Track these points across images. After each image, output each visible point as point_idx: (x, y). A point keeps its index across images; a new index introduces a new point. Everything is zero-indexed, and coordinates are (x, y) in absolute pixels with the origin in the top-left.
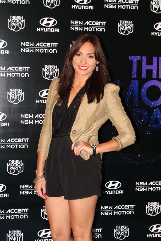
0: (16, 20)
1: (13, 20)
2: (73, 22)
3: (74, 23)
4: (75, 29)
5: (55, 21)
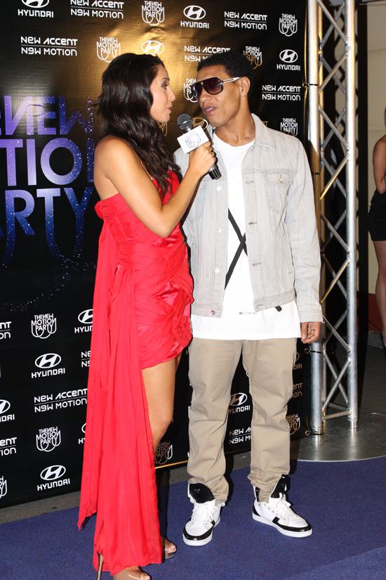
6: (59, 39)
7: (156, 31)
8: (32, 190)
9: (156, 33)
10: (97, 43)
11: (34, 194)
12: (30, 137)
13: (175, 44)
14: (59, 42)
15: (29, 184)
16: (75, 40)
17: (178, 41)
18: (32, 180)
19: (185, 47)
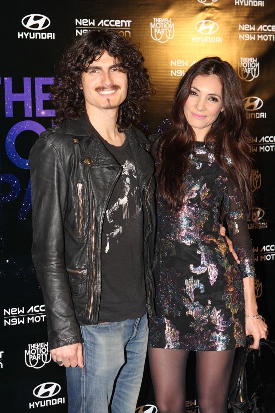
2: (80, 21)
3: (81, 24)
5: (47, 20)
6: (113, 21)
7: (210, 10)
9: (211, 12)
10: (152, 23)
13: (229, 23)
14: (113, 23)
16: (130, 21)
17: (233, 20)
19: (240, 26)
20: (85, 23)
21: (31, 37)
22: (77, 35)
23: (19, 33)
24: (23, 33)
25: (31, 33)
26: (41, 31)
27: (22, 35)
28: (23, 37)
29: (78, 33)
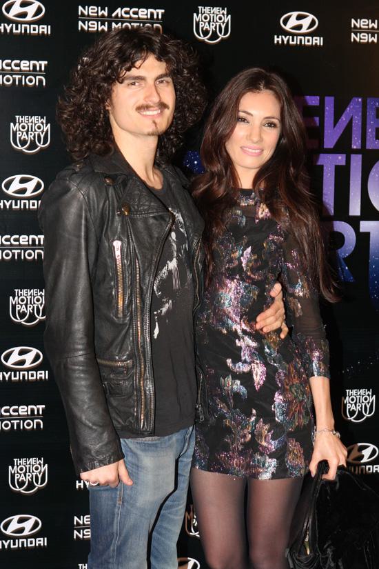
0: (212, 15)
1: (204, 15)
2: (357, 22)
4: (360, 39)
8: (354, 222)
11: (356, 227)
12: (356, 152)
15: (350, 214)
18: (355, 209)
20: (363, 25)
21: (291, 42)
22: (352, 40)
23: (276, 36)
24: (280, 36)
25: (291, 37)
26: (304, 35)
27: (280, 39)
28: (280, 42)
29: (354, 39)
